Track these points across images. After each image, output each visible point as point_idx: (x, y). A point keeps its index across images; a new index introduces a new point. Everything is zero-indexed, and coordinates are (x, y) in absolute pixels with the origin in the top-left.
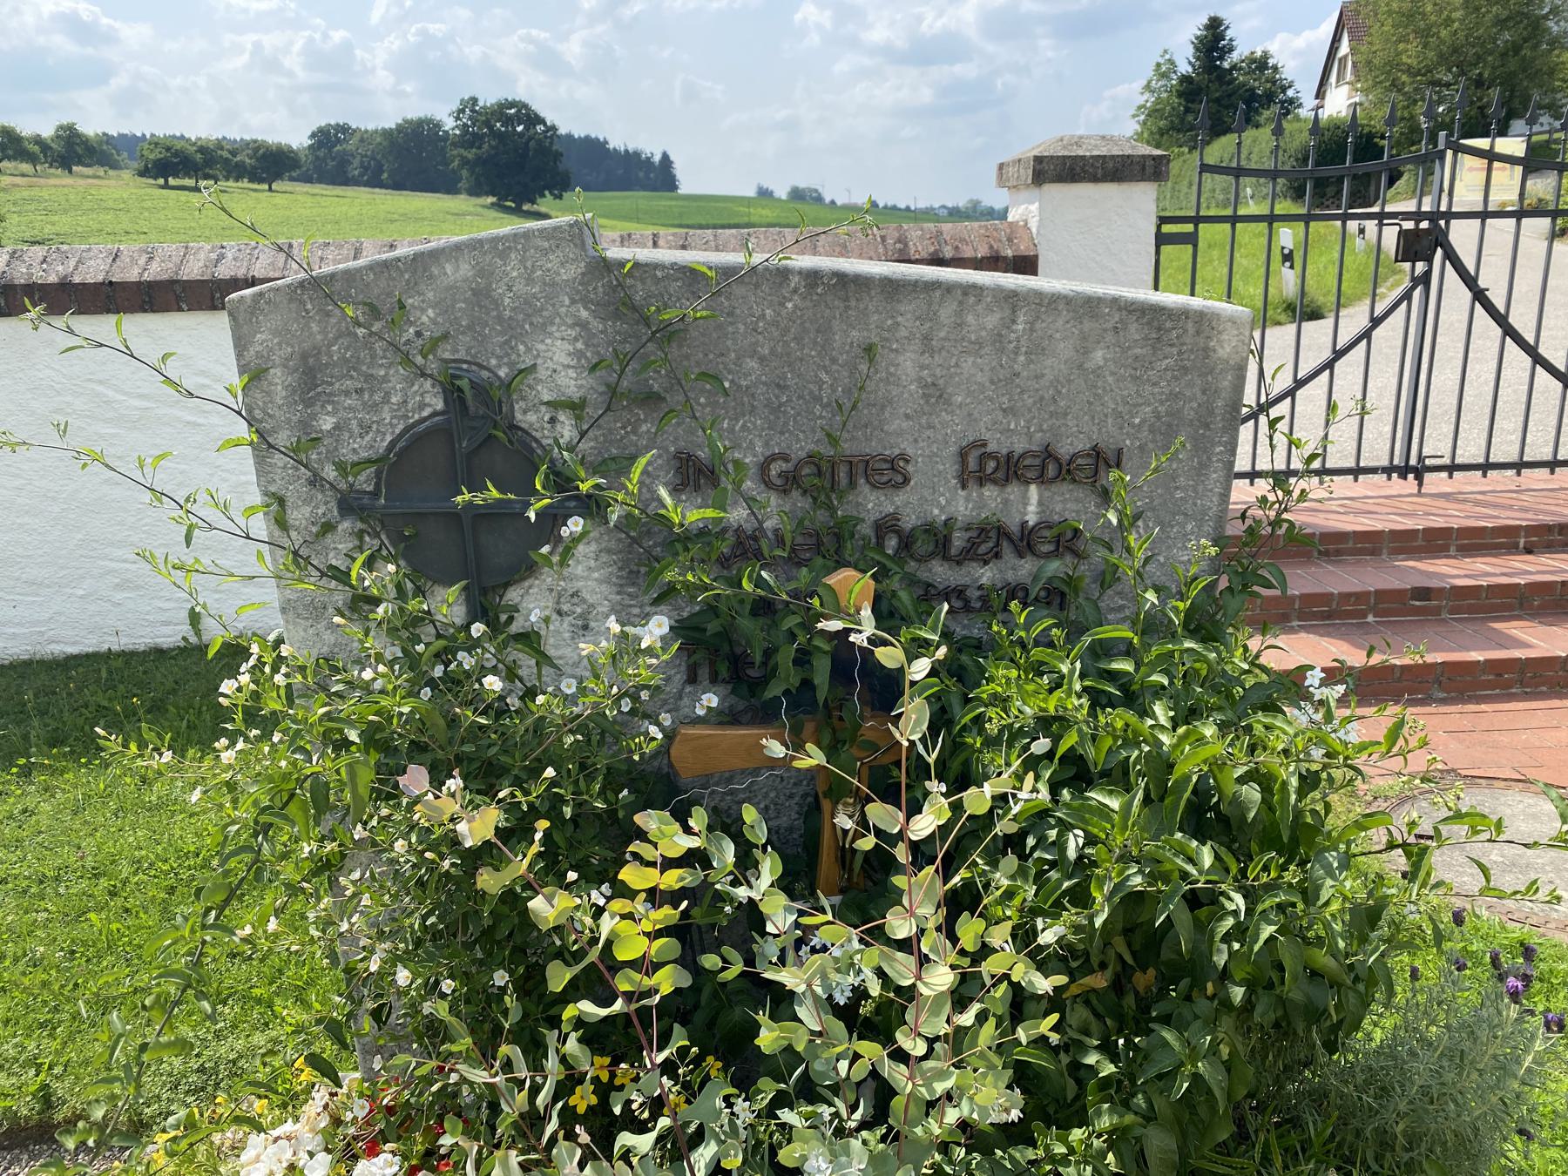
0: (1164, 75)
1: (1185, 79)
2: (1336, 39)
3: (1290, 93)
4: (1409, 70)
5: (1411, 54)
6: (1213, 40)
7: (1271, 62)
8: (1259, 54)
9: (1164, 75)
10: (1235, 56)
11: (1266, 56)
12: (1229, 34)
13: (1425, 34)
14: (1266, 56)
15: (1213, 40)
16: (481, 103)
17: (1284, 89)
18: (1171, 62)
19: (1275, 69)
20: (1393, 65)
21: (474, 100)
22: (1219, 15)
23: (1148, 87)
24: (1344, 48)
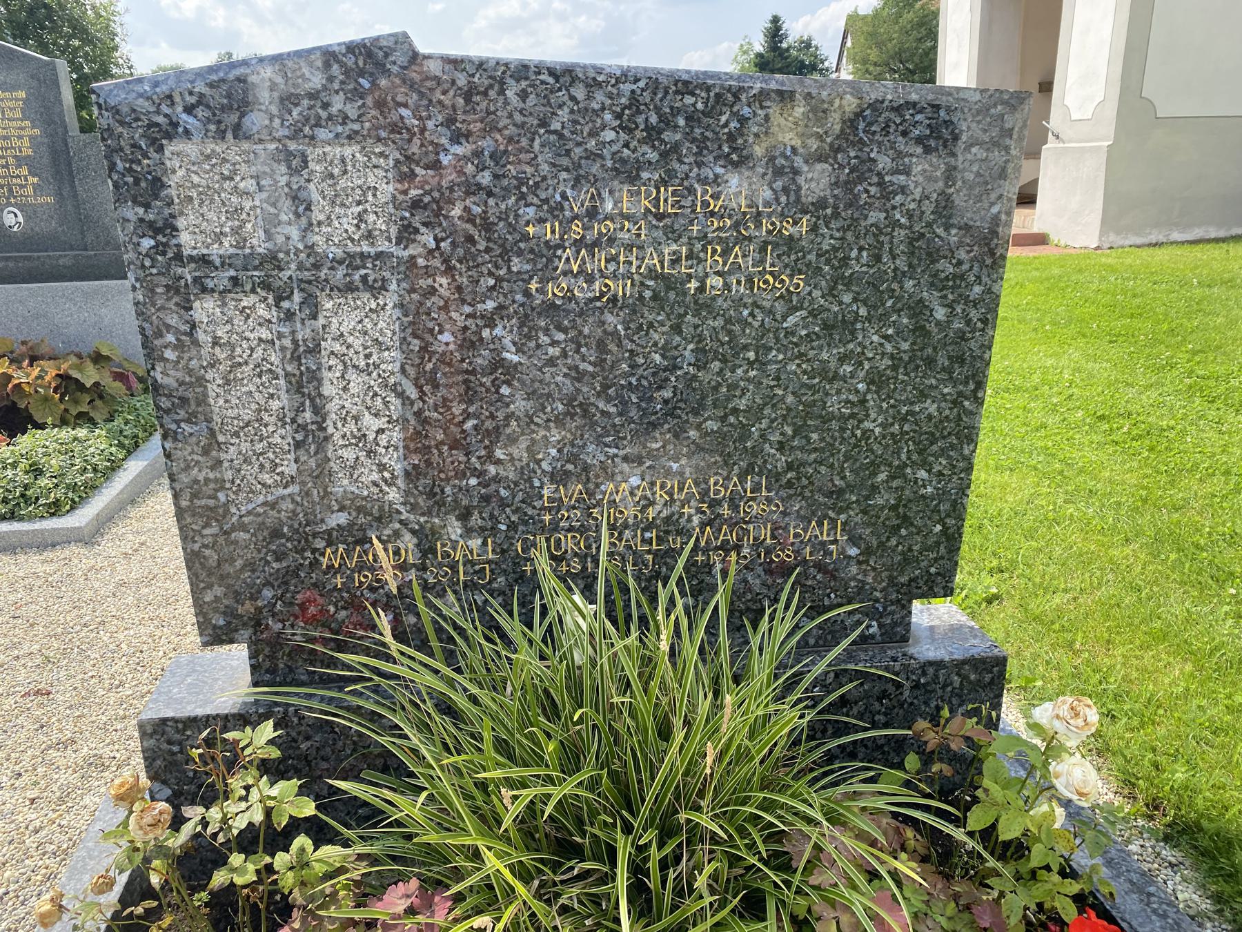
0: (745, 52)
1: (759, 55)
2: (845, 37)
3: (826, 64)
4: (875, 64)
5: (874, 55)
6: (775, 32)
7: (814, 43)
8: (805, 38)
9: (745, 52)
10: (790, 39)
11: (810, 39)
12: (785, 26)
13: (880, 45)
14: (810, 39)
15: (775, 32)
16: (235, 57)
17: (822, 62)
18: (749, 43)
19: (817, 48)
20: (865, 61)
21: (230, 55)
22: (779, 14)
23: (735, 59)
24: (849, 44)
